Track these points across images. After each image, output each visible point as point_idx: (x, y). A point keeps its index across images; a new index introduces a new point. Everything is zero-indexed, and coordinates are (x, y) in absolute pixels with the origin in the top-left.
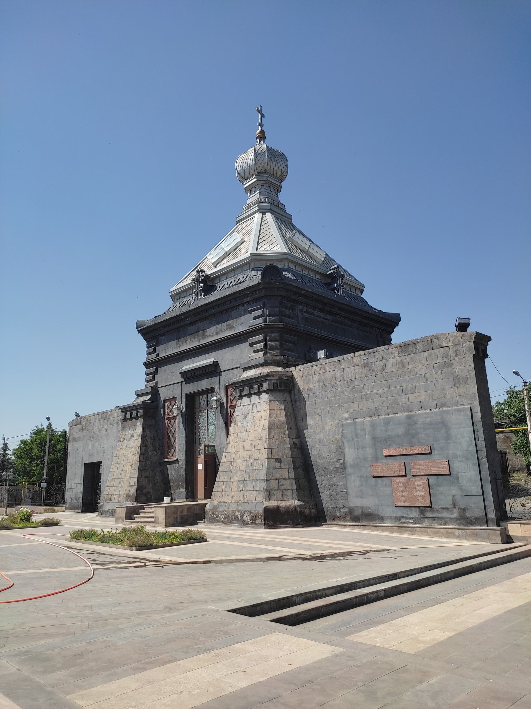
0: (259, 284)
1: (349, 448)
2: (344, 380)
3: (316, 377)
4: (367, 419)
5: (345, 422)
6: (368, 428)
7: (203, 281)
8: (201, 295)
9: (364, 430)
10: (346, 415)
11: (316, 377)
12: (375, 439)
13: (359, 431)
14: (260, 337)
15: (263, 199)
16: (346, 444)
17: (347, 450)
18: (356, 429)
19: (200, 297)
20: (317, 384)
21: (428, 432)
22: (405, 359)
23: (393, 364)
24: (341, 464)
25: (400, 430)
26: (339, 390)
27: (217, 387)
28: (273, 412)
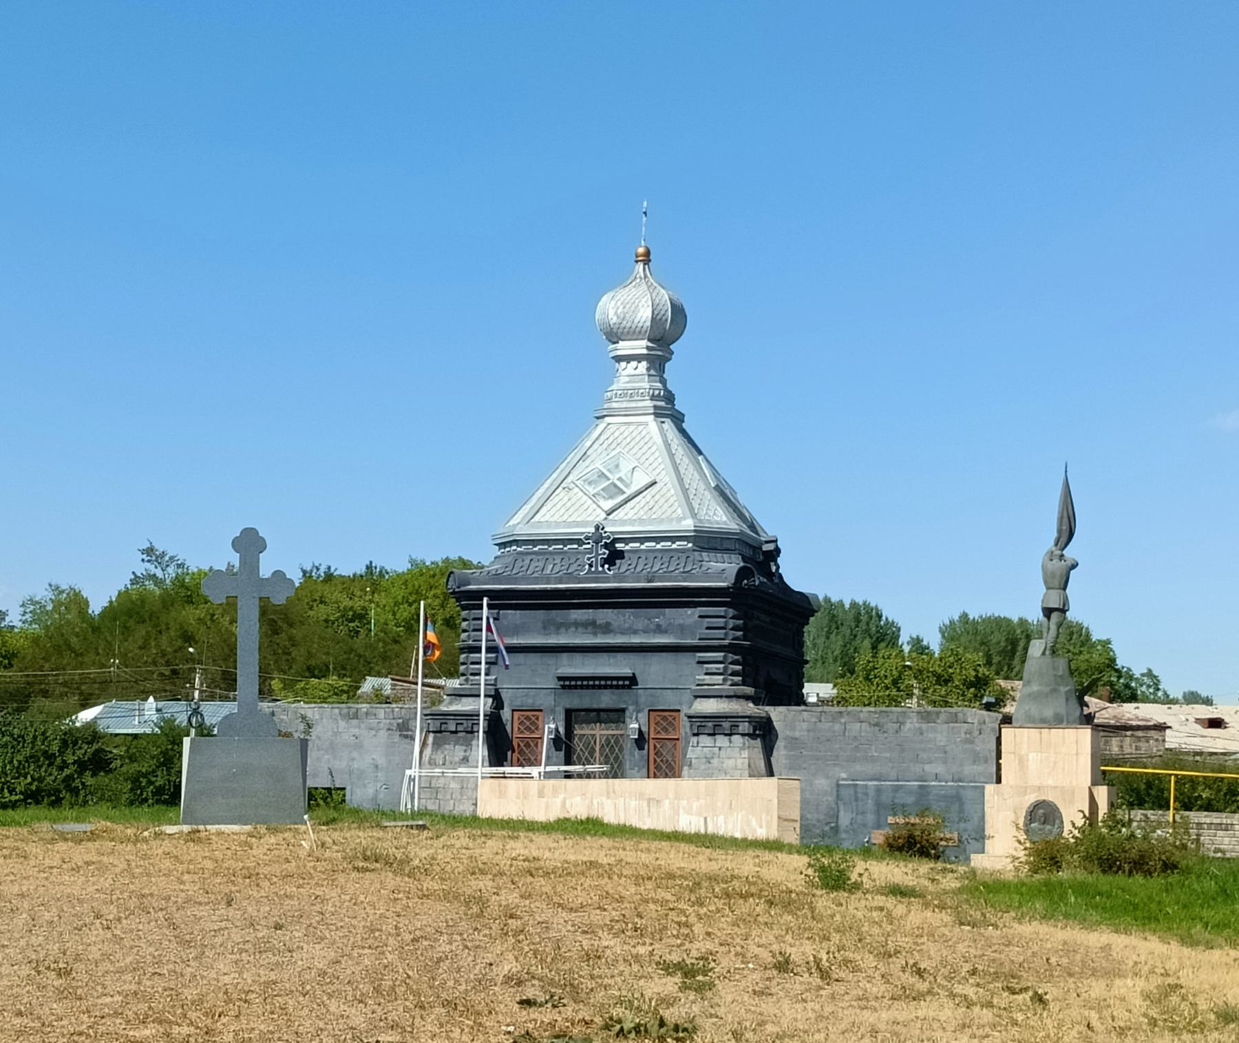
0: (728, 588)
1: (845, 811)
2: (844, 735)
3: (805, 725)
4: (870, 783)
5: (841, 782)
6: (872, 793)
7: (606, 546)
8: (602, 566)
9: (867, 794)
10: (844, 775)
11: (805, 725)
12: (879, 805)
13: (860, 795)
14: (719, 655)
15: (657, 392)
16: (841, 807)
17: (842, 814)
18: (856, 792)
19: (600, 569)
20: (806, 733)
21: (941, 804)
22: (924, 726)
23: (910, 729)
24: (832, 828)
25: (910, 800)
26: (837, 746)
27: (631, 708)
28: (752, 762)
